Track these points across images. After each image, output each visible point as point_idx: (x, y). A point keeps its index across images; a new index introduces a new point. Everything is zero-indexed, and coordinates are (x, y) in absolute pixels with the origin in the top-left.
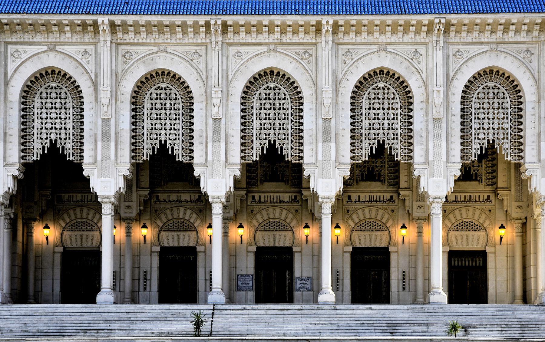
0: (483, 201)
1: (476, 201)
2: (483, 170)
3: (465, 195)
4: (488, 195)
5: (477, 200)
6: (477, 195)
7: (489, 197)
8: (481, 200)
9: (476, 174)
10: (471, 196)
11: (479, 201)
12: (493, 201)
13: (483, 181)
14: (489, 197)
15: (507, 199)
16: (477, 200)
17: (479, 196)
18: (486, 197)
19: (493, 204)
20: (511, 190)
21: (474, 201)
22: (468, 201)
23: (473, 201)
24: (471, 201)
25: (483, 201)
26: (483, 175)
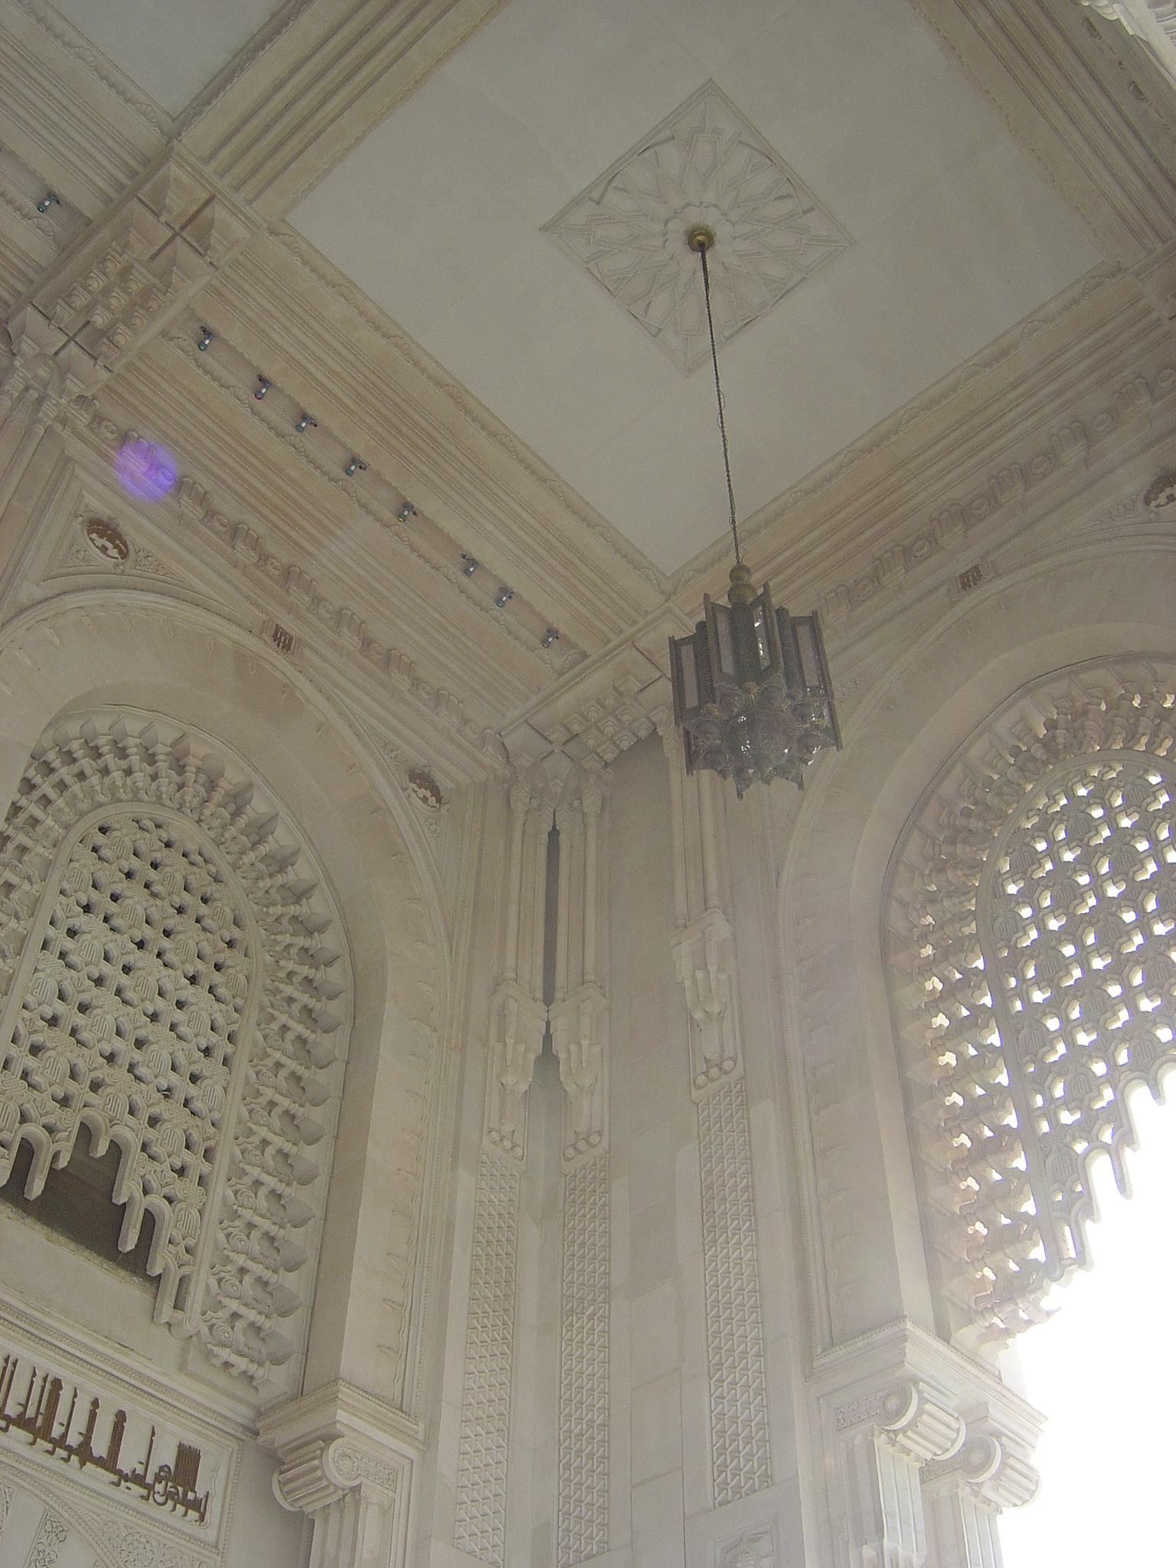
0: (138, 1479)
1: (84, 1453)
2: (215, 1211)
3: (16, 1350)
4: (192, 1440)
5: (100, 1446)
6: (112, 1400)
7: (188, 1459)
8: (127, 1461)
9: (150, 1221)
10: (57, 1384)
11: (109, 1463)
12: (214, 1509)
13: (196, 1298)
14: (188, 1459)
15: (386, 1512)
16: (100, 1446)
17: (121, 1417)
18: (166, 1456)
19: (211, 1536)
20: (428, 1444)
21: (73, 1440)
22: (22, 1422)
23: (60, 1442)
24: (44, 1433)
25: (138, 1479)
26: (205, 1253)
